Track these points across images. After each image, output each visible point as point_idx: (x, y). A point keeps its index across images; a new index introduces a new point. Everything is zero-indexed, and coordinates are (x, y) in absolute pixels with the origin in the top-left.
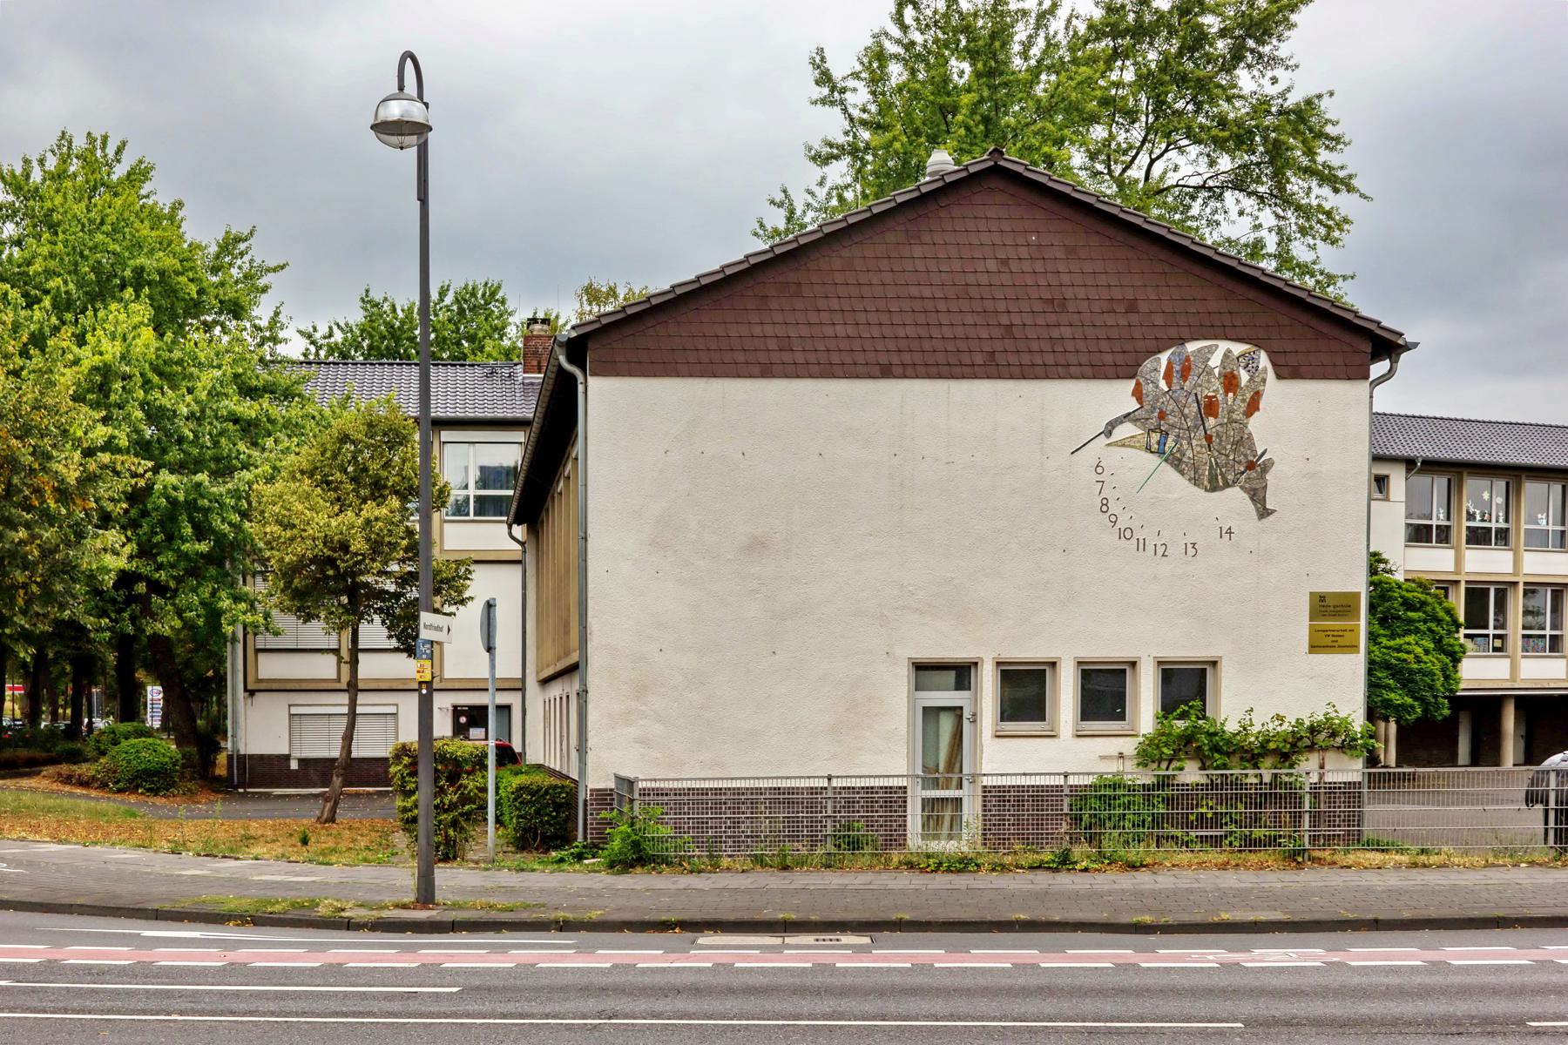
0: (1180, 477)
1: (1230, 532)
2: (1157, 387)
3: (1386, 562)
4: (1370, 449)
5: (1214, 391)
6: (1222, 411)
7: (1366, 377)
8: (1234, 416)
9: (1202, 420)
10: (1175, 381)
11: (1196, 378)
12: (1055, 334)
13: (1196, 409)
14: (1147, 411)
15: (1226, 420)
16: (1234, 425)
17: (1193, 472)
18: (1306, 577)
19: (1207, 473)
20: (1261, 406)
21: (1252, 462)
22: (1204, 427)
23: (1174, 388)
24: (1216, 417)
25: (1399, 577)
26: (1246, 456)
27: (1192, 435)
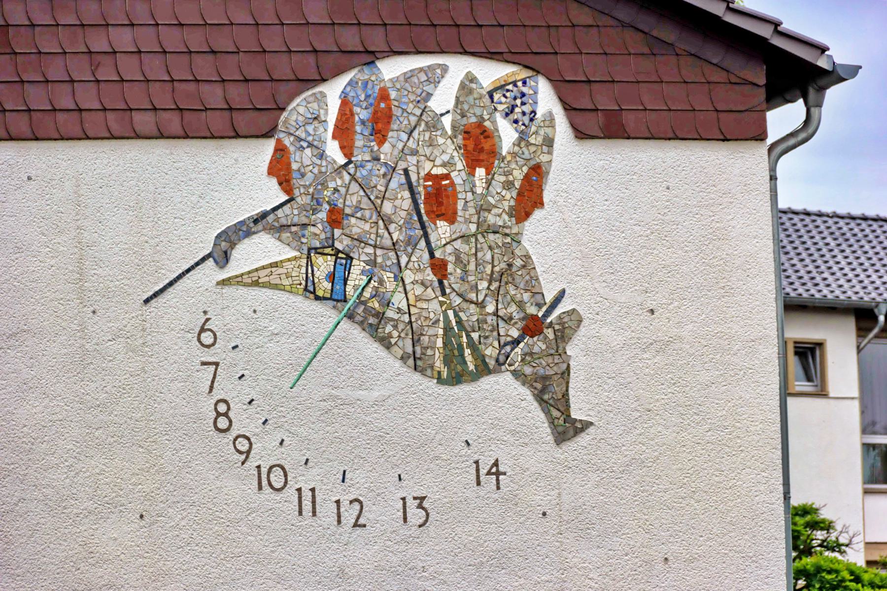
0: (382, 352)
1: (496, 471)
2: (322, 156)
3: (828, 526)
4: (780, 288)
5: (444, 165)
6: (465, 209)
7: (761, 136)
8: (491, 219)
9: (423, 227)
10: (359, 142)
11: (404, 137)
12: (99, 44)
13: (407, 204)
14: (303, 208)
15: (473, 228)
16: (491, 237)
17: (409, 342)
18: (660, 566)
19: (440, 343)
20: (547, 197)
21: (534, 318)
22: (428, 243)
23: (358, 158)
24: (451, 219)
25: (856, 557)
26: (521, 305)
27: (404, 260)
